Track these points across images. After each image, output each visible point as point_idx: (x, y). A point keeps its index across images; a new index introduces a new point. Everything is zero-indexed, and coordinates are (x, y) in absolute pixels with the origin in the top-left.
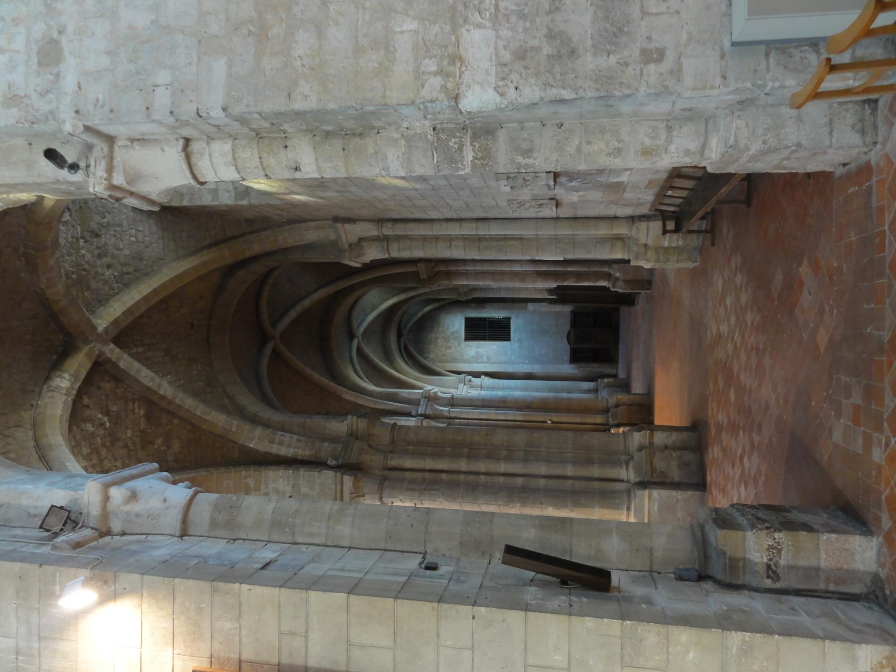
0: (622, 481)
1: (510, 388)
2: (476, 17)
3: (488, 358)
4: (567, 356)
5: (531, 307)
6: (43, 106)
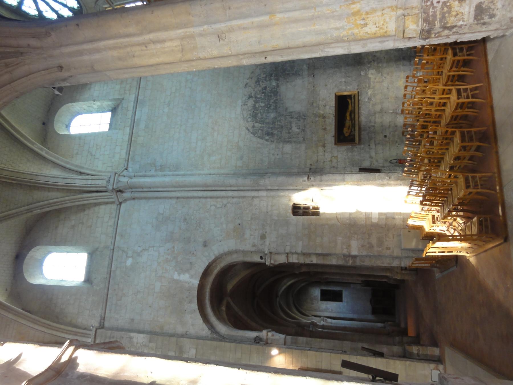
3: (332, 310)
5: (352, 286)
6: (261, 248)
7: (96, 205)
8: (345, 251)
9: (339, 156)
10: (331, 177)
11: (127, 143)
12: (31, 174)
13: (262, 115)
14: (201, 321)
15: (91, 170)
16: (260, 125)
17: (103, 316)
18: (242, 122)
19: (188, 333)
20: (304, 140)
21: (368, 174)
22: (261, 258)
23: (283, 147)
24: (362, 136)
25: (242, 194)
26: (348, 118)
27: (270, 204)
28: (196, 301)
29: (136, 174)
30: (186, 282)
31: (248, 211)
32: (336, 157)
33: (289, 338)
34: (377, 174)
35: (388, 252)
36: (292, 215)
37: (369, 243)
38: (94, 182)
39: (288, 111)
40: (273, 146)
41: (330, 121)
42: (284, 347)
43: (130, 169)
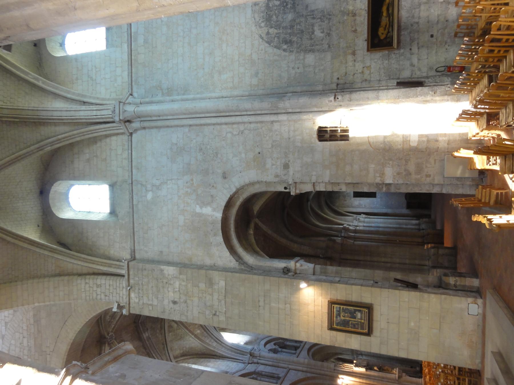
0: (426, 266)
1: (377, 222)
2: (388, 165)
3: (365, 206)
4: (405, 205)
6: (285, 178)
7: (107, 136)
8: (378, 180)
9: (372, 66)
10: (363, 94)
11: (127, 63)
12: (33, 110)
13: (277, 17)
15: (94, 98)
16: (276, 31)
17: (133, 248)
18: (254, 28)
19: (216, 265)
20: (329, 46)
21: (408, 89)
22: (285, 188)
23: (304, 59)
24: (402, 38)
25: (259, 118)
26: (385, 14)
27: (292, 128)
28: (221, 234)
29: (142, 100)
30: (209, 216)
31: (268, 138)
32: (369, 67)
33: (318, 267)
34: (419, 89)
35: (428, 180)
36: (317, 141)
37: (405, 170)
38: (99, 113)
39: (309, 9)
40: (293, 57)
41: (362, 19)
42: (312, 279)
43: (135, 94)
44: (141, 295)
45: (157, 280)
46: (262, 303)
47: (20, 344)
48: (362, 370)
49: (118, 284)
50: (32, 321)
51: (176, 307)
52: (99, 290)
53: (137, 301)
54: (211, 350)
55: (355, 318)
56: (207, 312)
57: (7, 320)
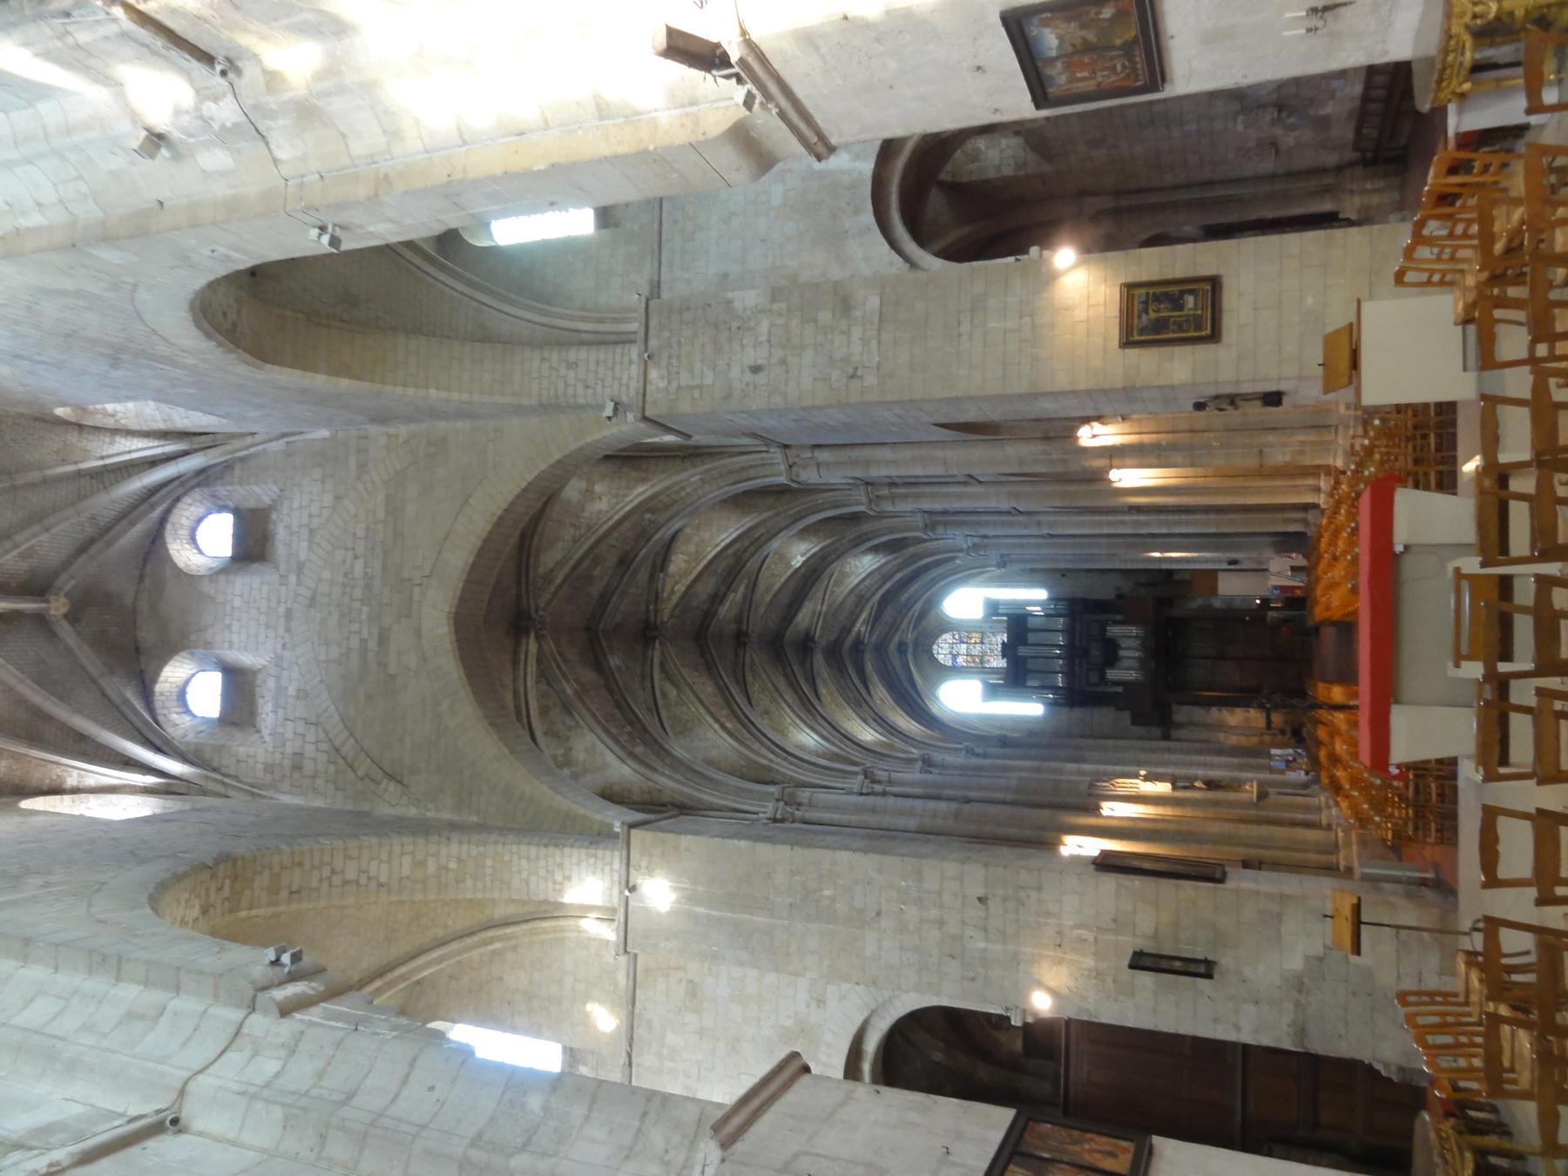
14: (886, 246)
44: (674, 369)
45: (716, 326)
46: (965, 328)
47: (345, 575)
48: (1163, 788)
49: (618, 358)
50: (381, 514)
51: (761, 379)
52: (571, 374)
53: (662, 384)
54: (763, 766)
55: (1181, 308)
56: (835, 374)
57: (316, 522)
